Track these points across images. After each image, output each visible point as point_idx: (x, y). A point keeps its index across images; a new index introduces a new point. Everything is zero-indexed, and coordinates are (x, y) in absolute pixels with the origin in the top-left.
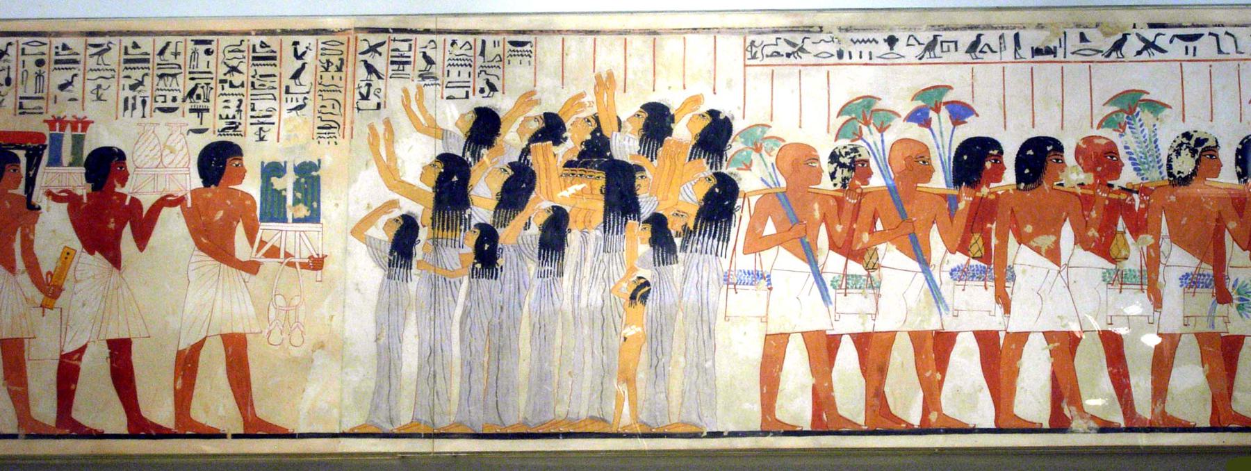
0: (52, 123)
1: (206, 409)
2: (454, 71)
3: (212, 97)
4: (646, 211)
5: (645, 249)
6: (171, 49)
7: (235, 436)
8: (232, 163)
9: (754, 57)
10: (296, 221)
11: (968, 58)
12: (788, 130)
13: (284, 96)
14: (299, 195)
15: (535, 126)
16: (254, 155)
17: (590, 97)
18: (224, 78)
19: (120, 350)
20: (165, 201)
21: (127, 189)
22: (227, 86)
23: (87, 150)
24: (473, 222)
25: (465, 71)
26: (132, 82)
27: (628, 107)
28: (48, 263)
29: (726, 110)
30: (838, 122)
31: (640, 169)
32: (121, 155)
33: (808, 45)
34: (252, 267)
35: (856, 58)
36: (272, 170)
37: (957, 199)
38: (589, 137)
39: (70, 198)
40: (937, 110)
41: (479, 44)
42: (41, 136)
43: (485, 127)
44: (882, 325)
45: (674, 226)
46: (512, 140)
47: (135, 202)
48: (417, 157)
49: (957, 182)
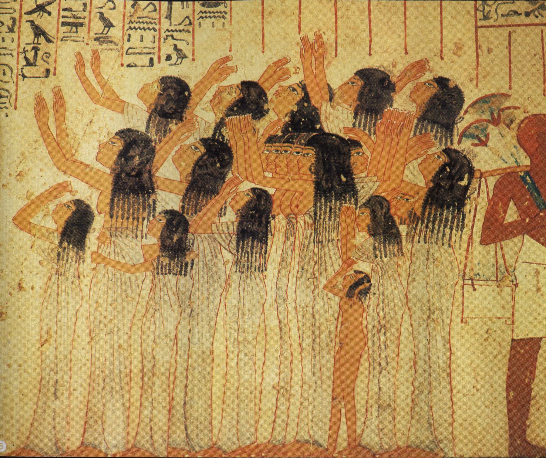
5: (362, 238)
9: (486, 17)
15: (230, 98)
25: (149, 35)
27: (340, 73)
31: (356, 144)
38: (295, 108)
45: (399, 212)
48: (94, 132)
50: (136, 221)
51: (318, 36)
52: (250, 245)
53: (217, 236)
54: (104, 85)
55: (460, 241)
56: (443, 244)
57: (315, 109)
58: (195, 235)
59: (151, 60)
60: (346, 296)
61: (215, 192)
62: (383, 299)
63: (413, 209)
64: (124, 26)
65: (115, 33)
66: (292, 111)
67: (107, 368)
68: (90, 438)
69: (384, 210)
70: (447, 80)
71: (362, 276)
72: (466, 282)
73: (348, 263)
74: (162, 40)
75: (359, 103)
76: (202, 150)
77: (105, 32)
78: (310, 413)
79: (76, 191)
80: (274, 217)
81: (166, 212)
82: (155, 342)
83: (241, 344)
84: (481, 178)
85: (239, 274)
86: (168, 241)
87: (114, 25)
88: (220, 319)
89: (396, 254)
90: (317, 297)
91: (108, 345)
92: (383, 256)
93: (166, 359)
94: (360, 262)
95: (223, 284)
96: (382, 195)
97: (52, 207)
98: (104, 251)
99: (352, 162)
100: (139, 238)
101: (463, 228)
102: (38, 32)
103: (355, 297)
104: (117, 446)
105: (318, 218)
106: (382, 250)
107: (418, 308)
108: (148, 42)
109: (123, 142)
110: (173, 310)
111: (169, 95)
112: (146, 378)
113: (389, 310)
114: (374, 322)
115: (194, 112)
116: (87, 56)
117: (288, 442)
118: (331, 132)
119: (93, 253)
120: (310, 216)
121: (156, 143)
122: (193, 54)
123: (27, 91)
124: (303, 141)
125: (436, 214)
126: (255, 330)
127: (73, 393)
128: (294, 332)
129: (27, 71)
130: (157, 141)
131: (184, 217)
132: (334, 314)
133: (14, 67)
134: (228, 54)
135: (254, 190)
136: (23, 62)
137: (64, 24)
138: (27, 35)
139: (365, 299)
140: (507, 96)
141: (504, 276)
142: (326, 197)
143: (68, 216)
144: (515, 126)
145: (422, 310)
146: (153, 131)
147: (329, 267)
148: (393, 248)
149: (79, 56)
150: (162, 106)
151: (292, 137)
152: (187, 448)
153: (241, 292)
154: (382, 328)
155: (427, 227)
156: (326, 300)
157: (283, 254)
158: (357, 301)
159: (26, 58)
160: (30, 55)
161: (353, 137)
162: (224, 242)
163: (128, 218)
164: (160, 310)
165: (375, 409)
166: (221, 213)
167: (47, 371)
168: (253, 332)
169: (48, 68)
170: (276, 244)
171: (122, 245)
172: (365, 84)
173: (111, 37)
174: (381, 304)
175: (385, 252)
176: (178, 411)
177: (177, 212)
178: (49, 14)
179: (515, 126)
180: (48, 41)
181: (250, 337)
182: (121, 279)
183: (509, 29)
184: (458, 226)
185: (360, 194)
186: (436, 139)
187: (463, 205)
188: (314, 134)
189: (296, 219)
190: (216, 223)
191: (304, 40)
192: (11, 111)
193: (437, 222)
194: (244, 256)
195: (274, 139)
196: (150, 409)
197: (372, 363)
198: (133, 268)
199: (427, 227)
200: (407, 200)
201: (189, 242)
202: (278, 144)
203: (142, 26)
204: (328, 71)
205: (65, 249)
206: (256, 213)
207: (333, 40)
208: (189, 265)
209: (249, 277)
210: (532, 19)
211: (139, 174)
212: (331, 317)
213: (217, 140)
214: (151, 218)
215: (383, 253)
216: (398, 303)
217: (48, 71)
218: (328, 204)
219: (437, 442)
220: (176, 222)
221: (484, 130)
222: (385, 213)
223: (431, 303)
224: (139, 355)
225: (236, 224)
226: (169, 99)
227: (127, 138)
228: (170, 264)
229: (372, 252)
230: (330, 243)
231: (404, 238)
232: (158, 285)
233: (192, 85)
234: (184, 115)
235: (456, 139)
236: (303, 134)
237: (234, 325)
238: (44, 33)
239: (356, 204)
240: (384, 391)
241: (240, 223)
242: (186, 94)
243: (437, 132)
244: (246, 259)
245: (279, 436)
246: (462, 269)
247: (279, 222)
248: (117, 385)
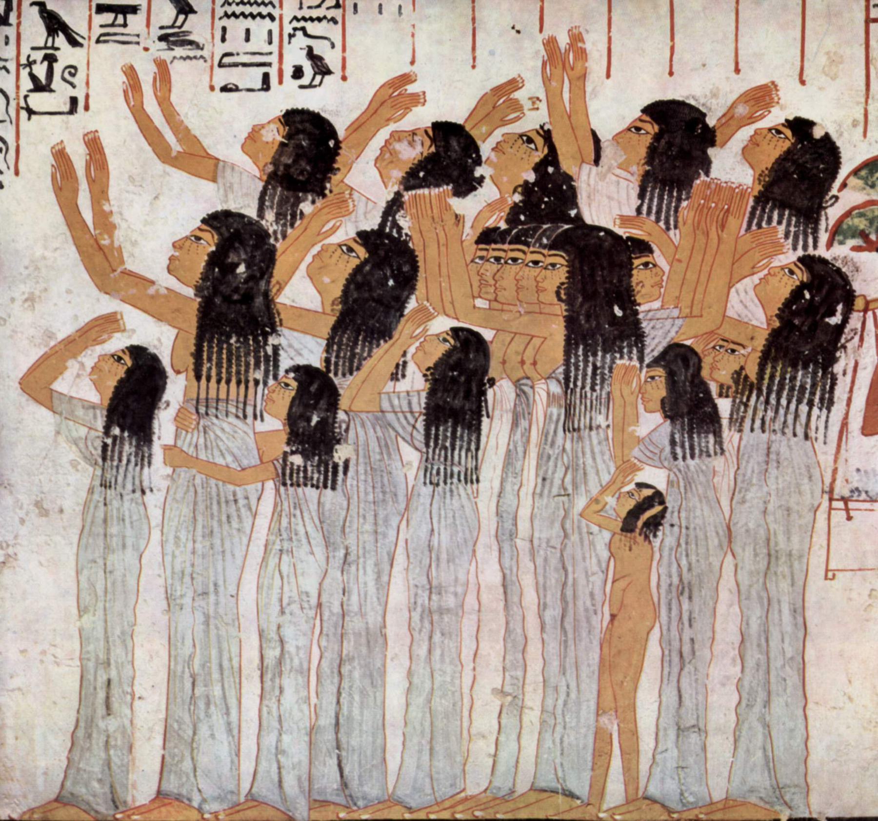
2: (237, 27)
4: (656, 341)
5: (652, 424)
15: (412, 153)
17: (533, 86)
24: (285, 363)
25: (260, 28)
27: (615, 106)
29: (828, 115)
31: (643, 247)
38: (531, 177)
43: (307, 154)
45: (717, 372)
46: (366, 185)
50: (243, 386)
52: (449, 434)
53: (390, 417)
55: (826, 427)
56: (795, 435)
57: (568, 179)
58: (351, 414)
59: (266, 77)
60: (622, 530)
61: (386, 333)
62: (687, 535)
63: (742, 368)
64: (213, 11)
66: (526, 182)
68: (172, 785)
69: (691, 371)
70: (810, 124)
71: (648, 492)
72: (835, 504)
73: (627, 468)
74: (286, 38)
75: (648, 168)
76: (362, 252)
77: (178, 23)
78: (558, 741)
79: (134, 331)
80: (492, 382)
81: (297, 369)
82: (283, 612)
83: (436, 617)
84: (865, 311)
85: (431, 488)
86: (302, 424)
87: (195, 8)
89: (712, 452)
90: (569, 531)
92: (688, 456)
93: (302, 641)
94: (647, 467)
96: (688, 343)
98: (186, 443)
99: (634, 281)
101: (831, 402)
103: (638, 531)
105: (571, 385)
106: (687, 445)
107: (749, 552)
108: (259, 42)
109: (216, 237)
110: (312, 553)
111: (299, 146)
112: (268, 677)
113: (698, 555)
114: (670, 576)
115: (346, 181)
118: (597, 224)
119: (166, 448)
120: (559, 381)
121: (276, 239)
122: (344, 67)
124: (545, 241)
125: (783, 378)
126: (460, 590)
128: (530, 598)
129: (38, 101)
130: (279, 236)
131: (330, 379)
132: (599, 562)
133: (12, 94)
134: (407, 69)
135: (455, 331)
136: (27, 84)
139: (655, 536)
142: (586, 346)
143: (118, 378)
145: (756, 555)
146: (270, 216)
149: (131, 72)
150: (287, 167)
151: (525, 233)
152: (341, 800)
153: (435, 520)
154: (684, 589)
155: (767, 402)
156: (585, 536)
157: (509, 451)
159: (33, 77)
160: (40, 71)
161: (637, 233)
162: (403, 428)
163: (228, 382)
166: (397, 374)
168: (456, 594)
169: (74, 95)
170: (496, 431)
171: (219, 433)
172: (661, 130)
173: (188, 33)
174: (684, 546)
175: (692, 448)
177: (317, 370)
181: (450, 601)
182: (218, 495)
184: (822, 399)
185: (647, 341)
186: (787, 236)
187: (834, 360)
188: (566, 227)
189: (532, 387)
190: (388, 393)
191: (550, 44)
193: (785, 394)
194: (440, 455)
195: (496, 236)
196: (276, 732)
197: (667, 652)
199: (767, 402)
200: (733, 351)
201: (340, 427)
202: (499, 246)
204: (593, 106)
205: (115, 438)
206: (460, 375)
208: (341, 469)
209: (448, 494)
211: (248, 298)
212: (595, 568)
213: (389, 236)
214: (271, 382)
215: (688, 451)
216: (714, 542)
217: (74, 101)
218: (591, 359)
219: (778, 789)
220: (315, 390)
222: (693, 376)
223: (772, 544)
225: (424, 395)
227: (224, 230)
228: (305, 467)
229: (668, 449)
230: (594, 433)
231: (725, 422)
232: (286, 505)
233: (341, 128)
234: (328, 185)
235: (824, 237)
236: (545, 226)
239: (641, 359)
241: (432, 393)
242: (331, 143)
243: (789, 224)
244: (442, 459)
245: (503, 783)
246: (828, 480)
247: (501, 395)
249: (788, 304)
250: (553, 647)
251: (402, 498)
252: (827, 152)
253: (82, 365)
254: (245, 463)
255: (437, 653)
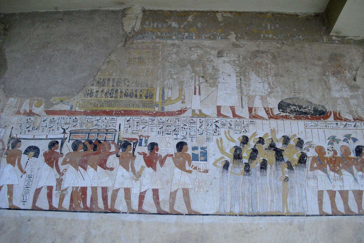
0: (140, 136)
1: (179, 207)
2: (237, 127)
3: (180, 131)
5: (286, 169)
6: (170, 120)
7: (186, 215)
8: (184, 147)
9: (307, 126)
10: (201, 161)
11: (354, 128)
12: (317, 143)
13: (197, 131)
14: (202, 155)
16: (190, 145)
17: (270, 134)
18: (183, 127)
19: (155, 192)
20: (167, 156)
21: (159, 153)
22: (183, 129)
23: (149, 142)
25: (239, 127)
26: (160, 127)
27: (279, 136)
28: (137, 169)
29: (302, 138)
30: (328, 141)
31: (284, 150)
32: (157, 144)
33: (318, 124)
34: (190, 172)
35: (330, 128)
36: (195, 148)
37: (357, 159)
39: (144, 154)
40: (349, 139)
41: (242, 122)
42: (136, 139)
43: (245, 140)
44: (345, 189)
45: (293, 164)
46: (252, 143)
47: (160, 156)
49: (357, 155)
51: (274, 129)
53: (256, 168)
54: (231, 137)
61: (255, 159)
65: (232, 127)
67: (234, 195)
68: (232, 210)
71: (287, 177)
72: (308, 179)
73: (284, 174)
76: (252, 151)
80: (268, 165)
81: (245, 163)
82: (244, 190)
83: (263, 191)
88: (258, 186)
91: (234, 191)
95: (258, 178)
97: (221, 162)
98: (232, 171)
100: (240, 168)
102: (217, 126)
104: (238, 212)
107: (299, 184)
108: (239, 129)
112: (243, 198)
116: (227, 131)
117: (274, 211)
119: (230, 171)
123: (215, 138)
127: (227, 200)
128: (273, 188)
129: (215, 134)
137: (222, 125)
138: (214, 127)
140: (313, 142)
141: (315, 177)
144: (314, 148)
147: (280, 175)
148: (292, 172)
150: (243, 141)
152: (253, 212)
154: (292, 188)
157: (270, 173)
158: (286, 182)
160: (215, 131)
161: (283, 149)
164: (245, 184)
165: (291, 205)
167: (222, 196)
168: (265, 188)
176: (250, 204)
178: (219, 123)
179: (314, 148)
180: (219, 128)
181: (264, 189)
183: (312, 129)
187: (306, 163)
191: (271, 129)
192: (211, 142)
198: (239, 174)
203: (238, 125)
207: (277, 130)
210: (315, 127)
211: (239, 155)
214: (242, 164)
216: (294, 183)
219: (305, 212)
220: (247, 165)
221: (308, 148)
224: (241, 193)
226: (244, 140)
231: (294, 169)
233: (249, 138)
235: (303, 150)
237: (261, 187)
238: (218, 127)
240: (293, 201)
241: (261, 166)
245: (272, 210)
247: (269, 166)
248: (237, 199)
249: (300, 157)
250: (277, 194)
251: (258, 177)
252: (302, 141)
253: (220, 162)
254: (239, 173)
255: (263, 195)
